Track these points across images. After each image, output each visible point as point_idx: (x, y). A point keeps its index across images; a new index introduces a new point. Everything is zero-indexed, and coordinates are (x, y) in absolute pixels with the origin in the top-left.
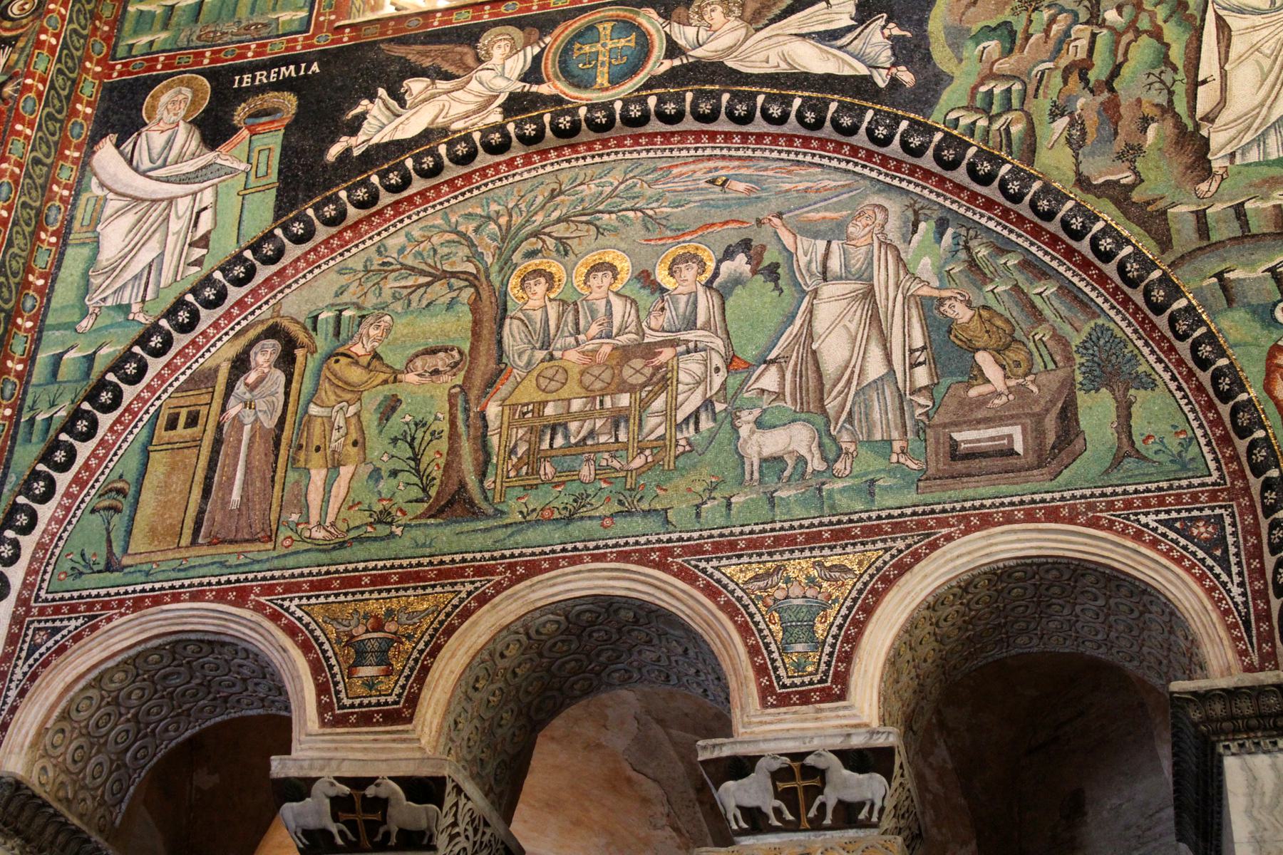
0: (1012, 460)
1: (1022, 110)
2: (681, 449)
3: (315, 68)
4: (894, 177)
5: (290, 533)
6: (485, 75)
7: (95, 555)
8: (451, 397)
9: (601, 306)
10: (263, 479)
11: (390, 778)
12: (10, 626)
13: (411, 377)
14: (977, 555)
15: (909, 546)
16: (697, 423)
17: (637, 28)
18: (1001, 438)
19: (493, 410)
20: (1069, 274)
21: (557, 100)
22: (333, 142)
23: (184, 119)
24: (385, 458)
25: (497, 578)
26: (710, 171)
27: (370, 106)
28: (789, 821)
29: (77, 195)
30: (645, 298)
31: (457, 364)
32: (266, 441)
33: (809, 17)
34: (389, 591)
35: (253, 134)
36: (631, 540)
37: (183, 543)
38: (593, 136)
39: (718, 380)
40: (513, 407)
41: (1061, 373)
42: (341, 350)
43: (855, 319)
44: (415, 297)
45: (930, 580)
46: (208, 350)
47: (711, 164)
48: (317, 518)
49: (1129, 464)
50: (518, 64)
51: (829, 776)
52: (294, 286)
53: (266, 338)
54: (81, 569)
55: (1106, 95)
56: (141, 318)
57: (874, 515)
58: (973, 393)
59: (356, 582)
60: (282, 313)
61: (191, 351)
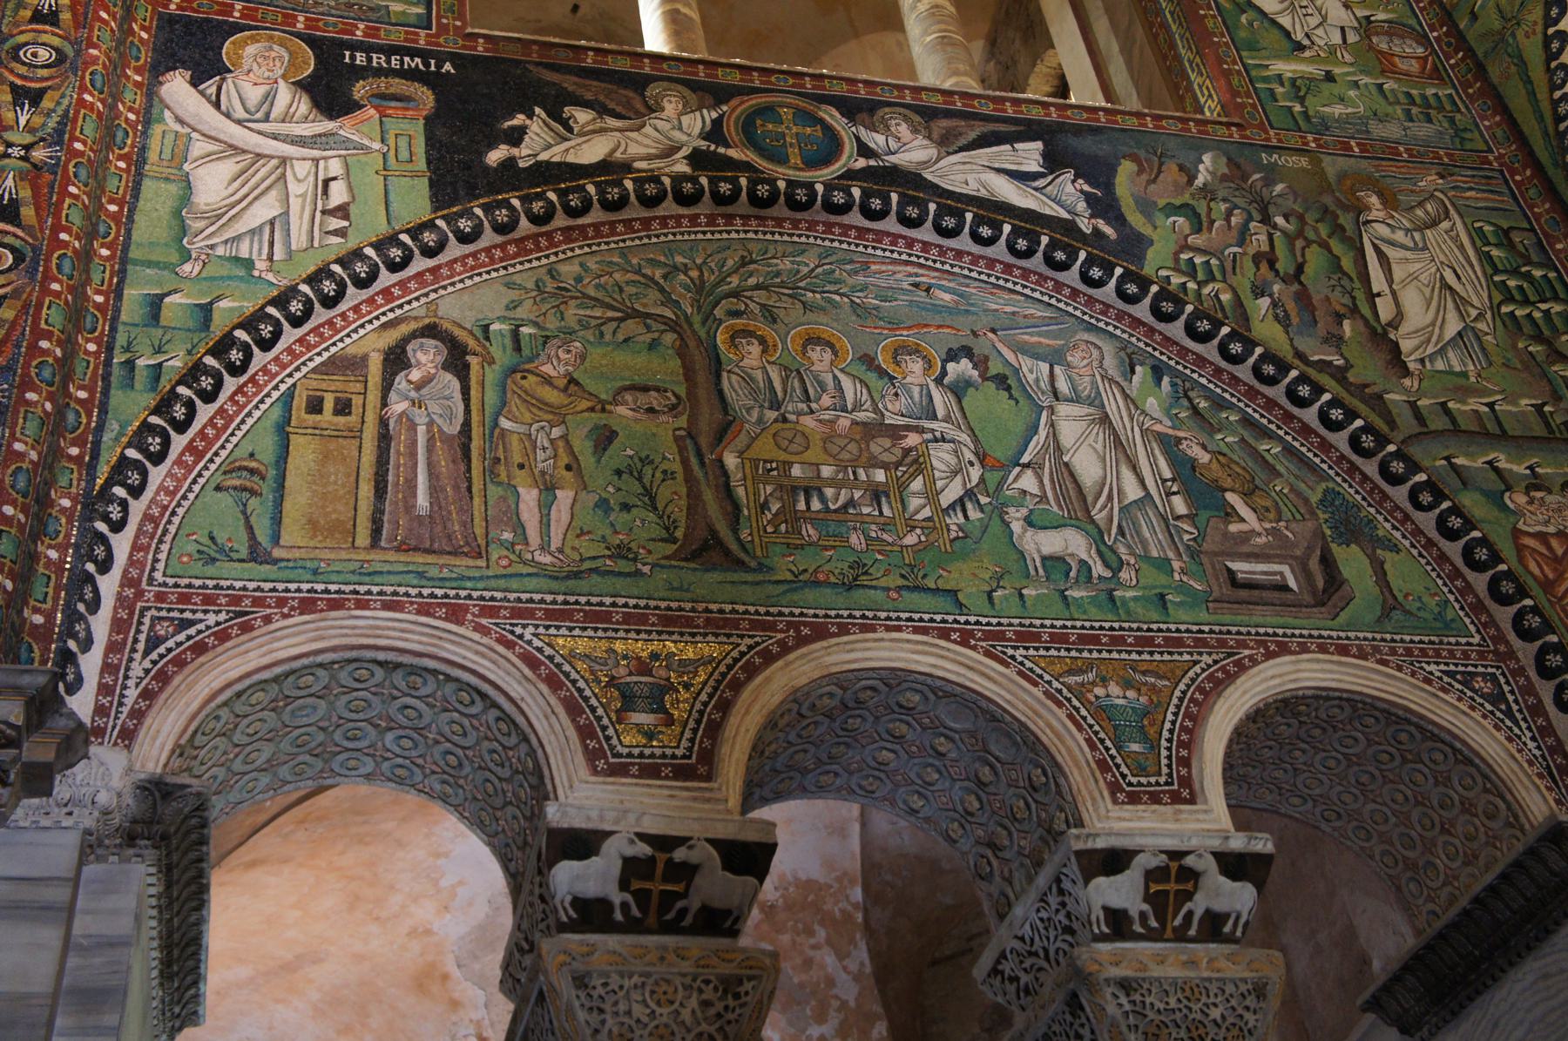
0: (1289, 596)
1: (1224, 281)
2: (953, 535)
3: (448, 67)
4: (1098, 320)
5: (505, 553)
6: (659, 124)
7: (230, 540)
8: (677, 439)
9: (829, 379)
10: (456, 488)
11: (708, 840)
12: (115, 608)
13: (622, 410)
14: (1286, 678)
15: (1216, 662)
16: (964, 511)
17: (821, 121)
18: (1275, 573)
19: (731, 461)
20: (1289, 438)
21: (747, 167)
22: (492, 146)
23: (284, 77)
24: (611, 489)
25: (780, 636)
26: (910, 275)
27: (528, 122)
28: (1154, 929)
29: (147, 123)
30: (871, 377)
31: (673, 408)
32: (451, 447)
33: (1000, 154)
34: (649, 633)
35: (383, 115)
36: (926, 617)
37: (359, 542)
38: (787, 213)
39: (975, 473)
40: (755, 462)
41: (1310, 525)
42: (527, 367)
43: (1098, 438)
44: (608, 329)
45: (1248, 696)
46: (348, 335)
47: (909, 269)
48: (539, 541)
49: (1397, 615)
50: (695, 123)
51: (1203, 881)
52: (450, 289)
53: (423, 336)
54: (213, 554)
55: (1296, 287)
56: (270, 277)
57: (1173, 627)
58: (1234, 528)
59: (605, 617)
60: (440, 314)
61: (326, 331)
